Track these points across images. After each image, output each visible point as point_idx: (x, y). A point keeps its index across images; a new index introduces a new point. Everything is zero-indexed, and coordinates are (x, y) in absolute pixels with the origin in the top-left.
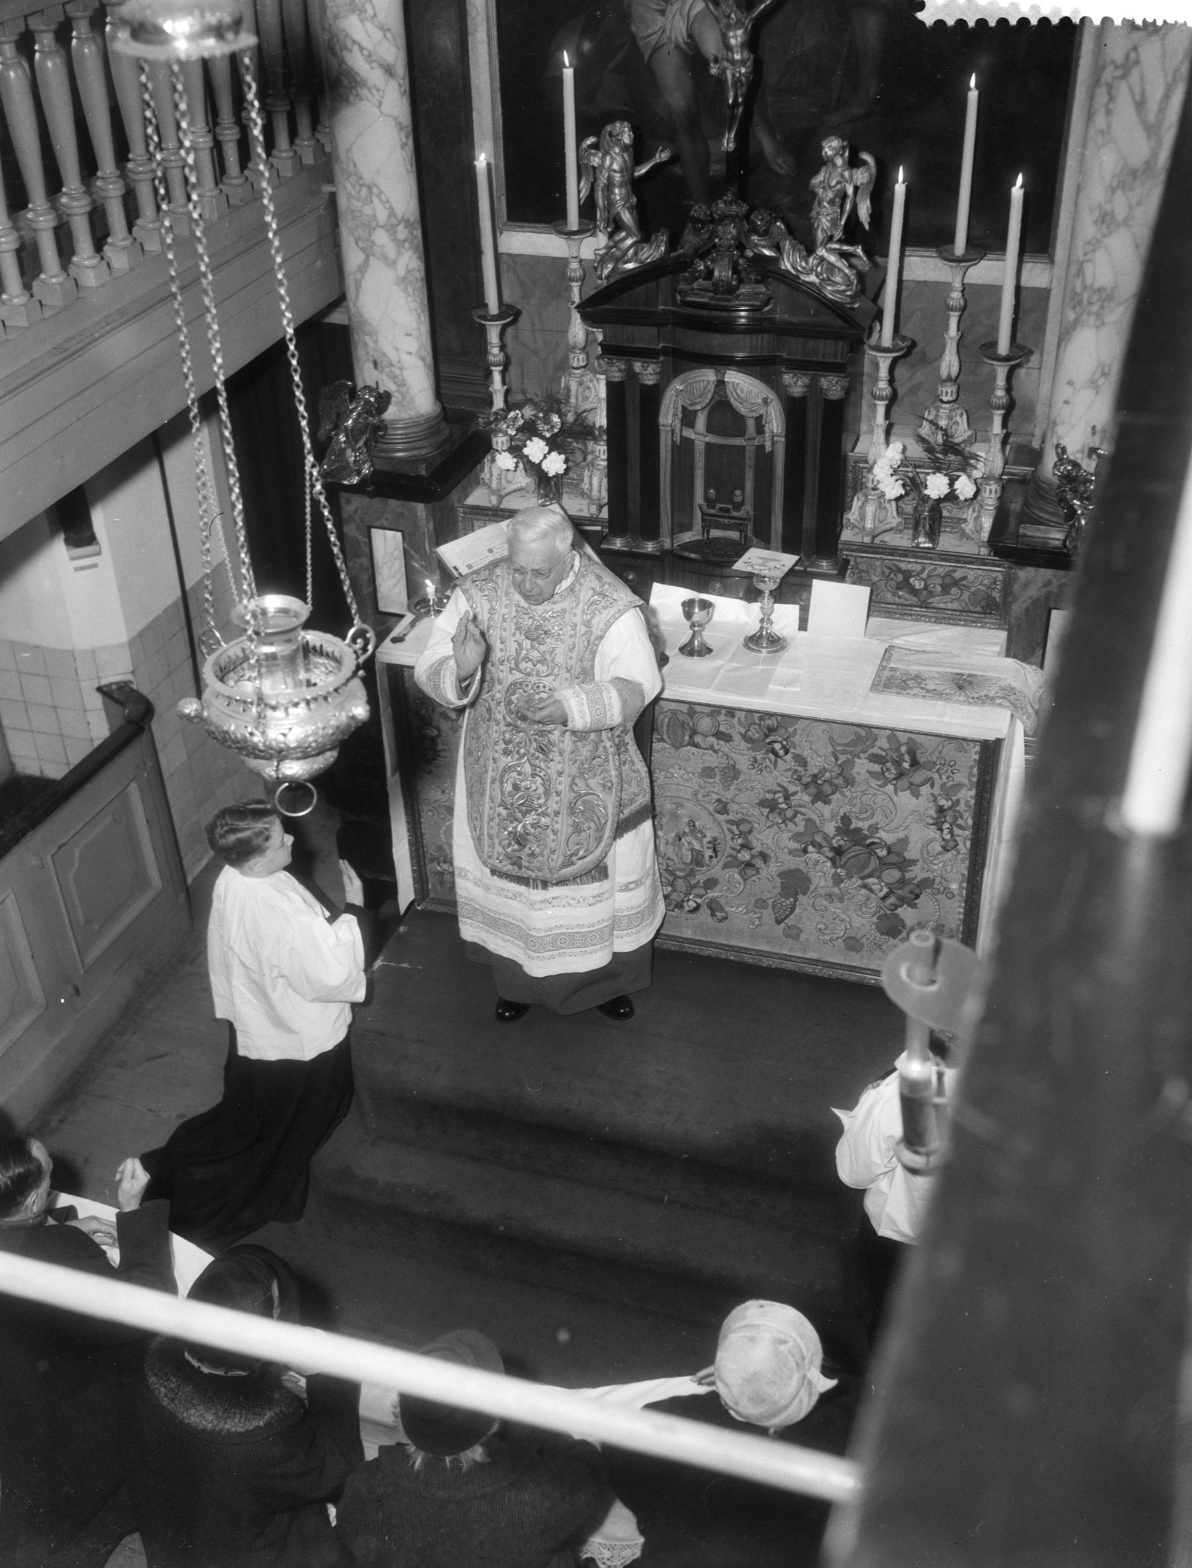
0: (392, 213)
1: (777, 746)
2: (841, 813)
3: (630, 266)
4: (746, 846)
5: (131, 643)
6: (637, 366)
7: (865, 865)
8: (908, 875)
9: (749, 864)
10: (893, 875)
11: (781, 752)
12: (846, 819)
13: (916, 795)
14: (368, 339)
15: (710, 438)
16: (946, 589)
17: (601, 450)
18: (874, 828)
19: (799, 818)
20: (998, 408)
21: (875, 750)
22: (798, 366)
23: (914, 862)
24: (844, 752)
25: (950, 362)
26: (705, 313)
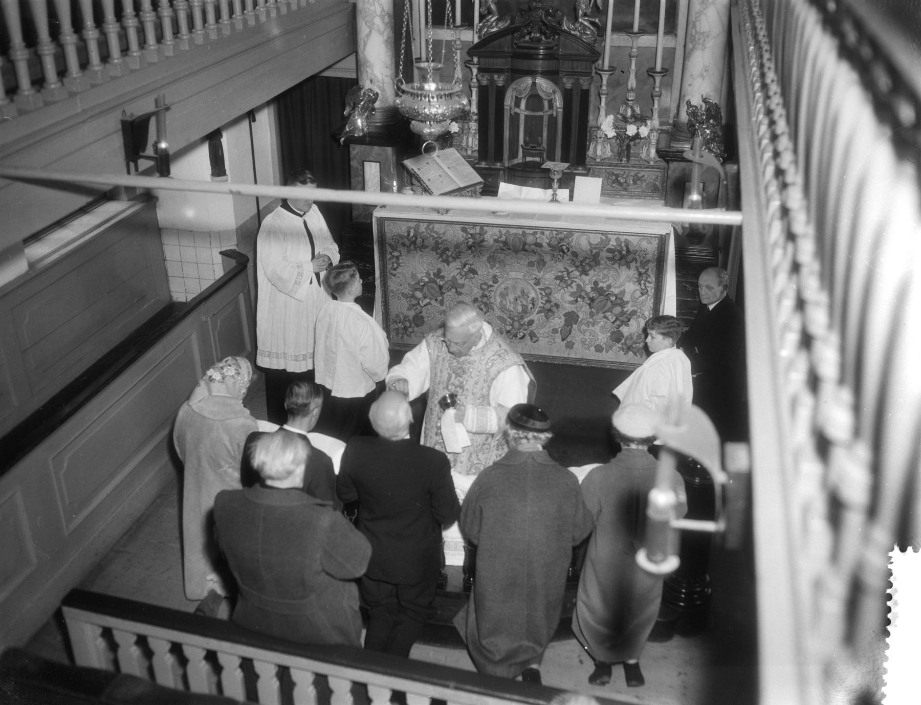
0: (383, 10)
1: (564, 247)
3: (495, 29)
4: (548, 301)
5: (237, 230)
6: (496, 77)
7: (605, 305)
8: (625, 309)
9: (550, 310)
10: (618, 310)
12: (596, 283)
13: (629, 268)
14: (368, 69)
15: (527, 113)
16: (635, 182)
17: (474, 126)
18: (609, 286)
19: (574, 285)
21: (610, 246)
23: (627, 302)
24: (595, 248)
25: (632, 82)
26: (527, 51)
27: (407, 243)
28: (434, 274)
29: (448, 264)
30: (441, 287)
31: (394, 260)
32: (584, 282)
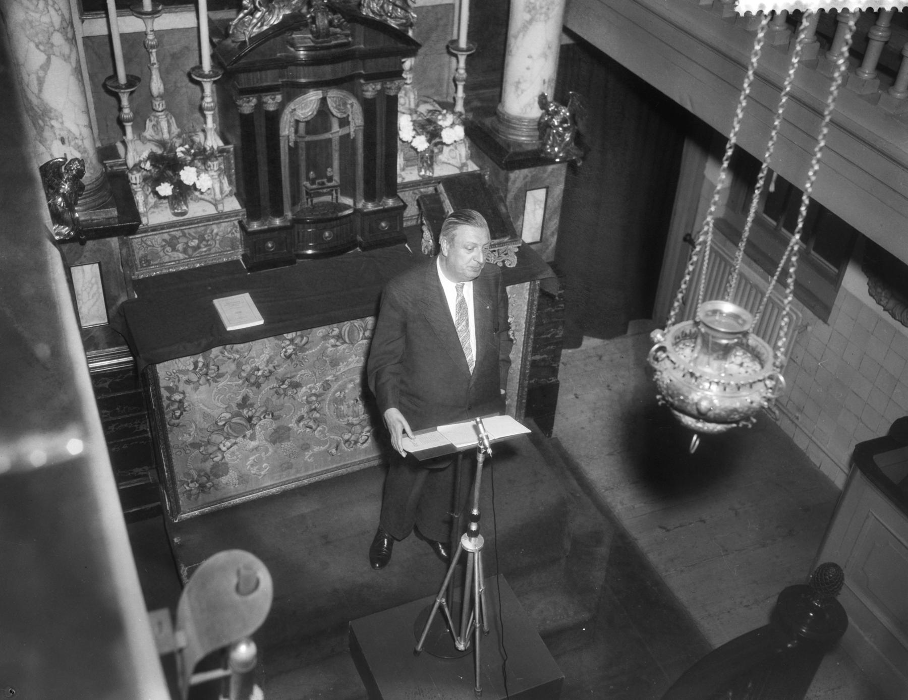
20: (462, 81)
22: (371, 78)
27: (194, 378)
28: (239, 405)
29: (258, 385)
30: (250, 419)
31: (176, 406)
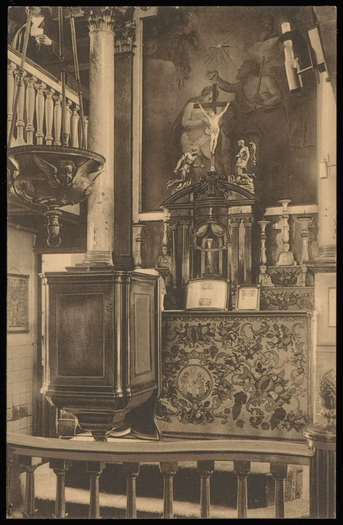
1: (232, 335)
2: (257, 363)
8: (286, 388)
10: (279, 389)
11: (234, 338)
13: (286, 350)
32: (249, 365)
